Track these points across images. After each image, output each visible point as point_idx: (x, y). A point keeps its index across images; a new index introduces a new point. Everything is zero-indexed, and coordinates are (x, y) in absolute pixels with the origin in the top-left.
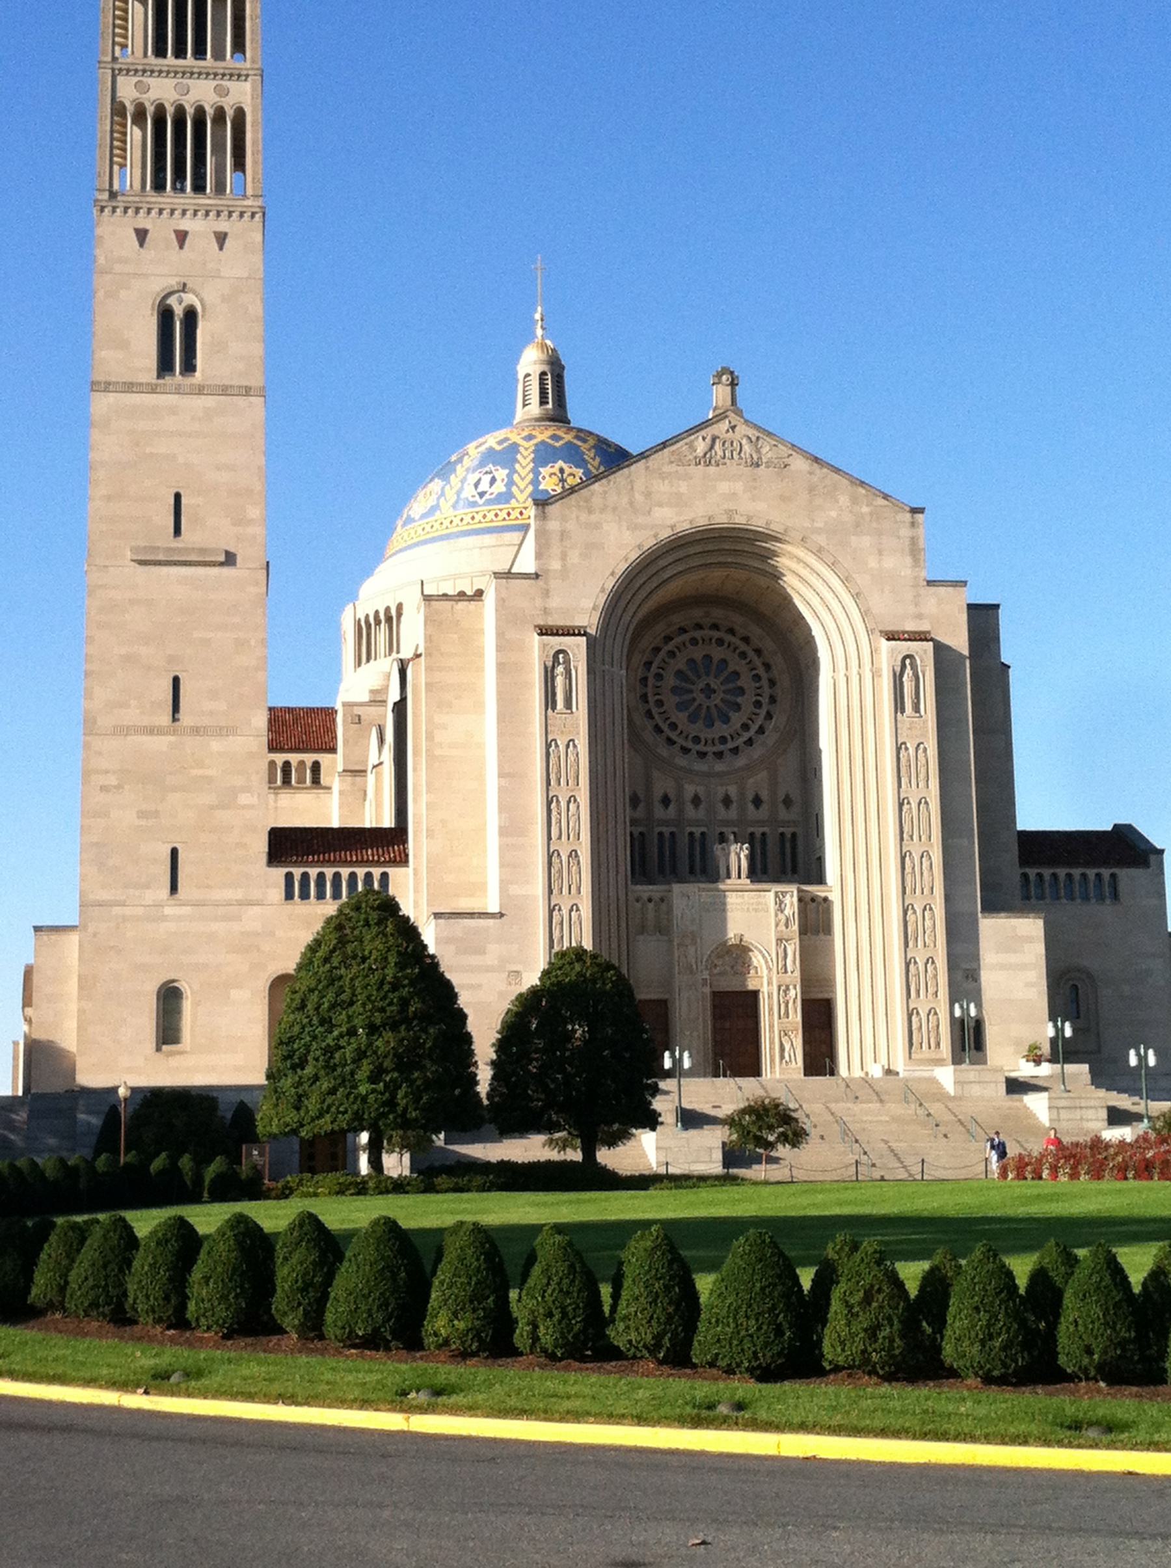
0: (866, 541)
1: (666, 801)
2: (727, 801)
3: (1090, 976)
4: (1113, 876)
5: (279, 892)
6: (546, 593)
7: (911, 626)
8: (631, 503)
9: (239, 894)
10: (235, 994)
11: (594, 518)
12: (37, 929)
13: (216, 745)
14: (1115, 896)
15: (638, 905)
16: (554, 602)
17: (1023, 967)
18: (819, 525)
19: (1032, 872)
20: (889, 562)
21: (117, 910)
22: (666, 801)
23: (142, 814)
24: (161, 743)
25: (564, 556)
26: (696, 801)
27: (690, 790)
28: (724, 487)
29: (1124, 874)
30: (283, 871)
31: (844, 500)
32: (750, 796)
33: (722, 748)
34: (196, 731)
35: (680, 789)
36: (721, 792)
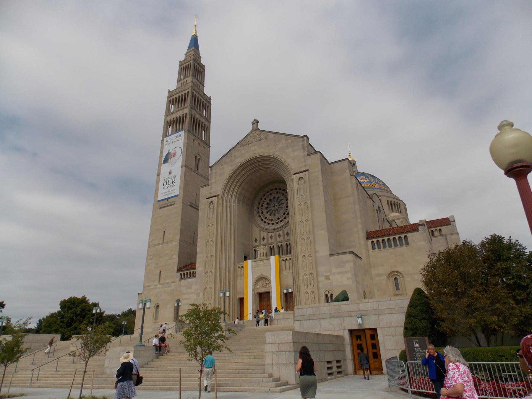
0: (290, 150)
1: (264, 239)
2: (279, 236)
3: (400, 273)
4: (406, 237)
5: (178, 279)
6: (211, 189)
7: (303, 169)
8: (231, 160)
9: (171, 280)
10: (168, 306)
11: (222, 167)
12: (139, 294)
13: (170, 245)
14: (407, 244)
15: (239, 269)
16: (213, 190)
17: (346, 272)
18: (277, 149)
19: (375, 240)
20: (296, 153)
21: (149, 288)
22: (264, 239)
23: (156, 264)
24: (160, 247)
25: (215, 178)
26: (271, 237)
27: (270, 234)
28: (253, 148)
29: (409, 235)
30: (179, 273)
31: (283, 141)
32: (285, 233)
33: (278, 221)
34: (167, 242)
35: (267, 235)
36: (278, 233)
